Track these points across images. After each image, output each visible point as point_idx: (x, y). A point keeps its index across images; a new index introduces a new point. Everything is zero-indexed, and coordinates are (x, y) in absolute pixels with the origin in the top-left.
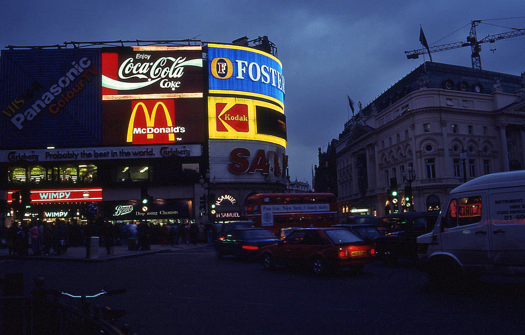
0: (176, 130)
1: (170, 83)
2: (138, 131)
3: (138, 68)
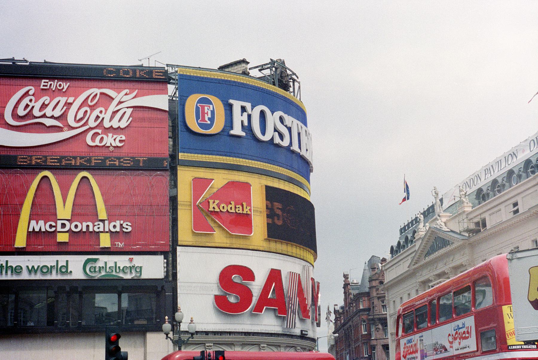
0: (115, 227)
2: (41, 226)
3: (44, 106)
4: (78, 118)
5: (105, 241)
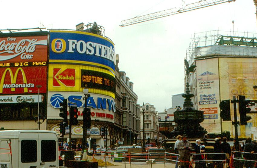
0: (29, 85)
1: (26, 55)
3: (8, 47)
4: (18, 50)
5: (26, 90)
